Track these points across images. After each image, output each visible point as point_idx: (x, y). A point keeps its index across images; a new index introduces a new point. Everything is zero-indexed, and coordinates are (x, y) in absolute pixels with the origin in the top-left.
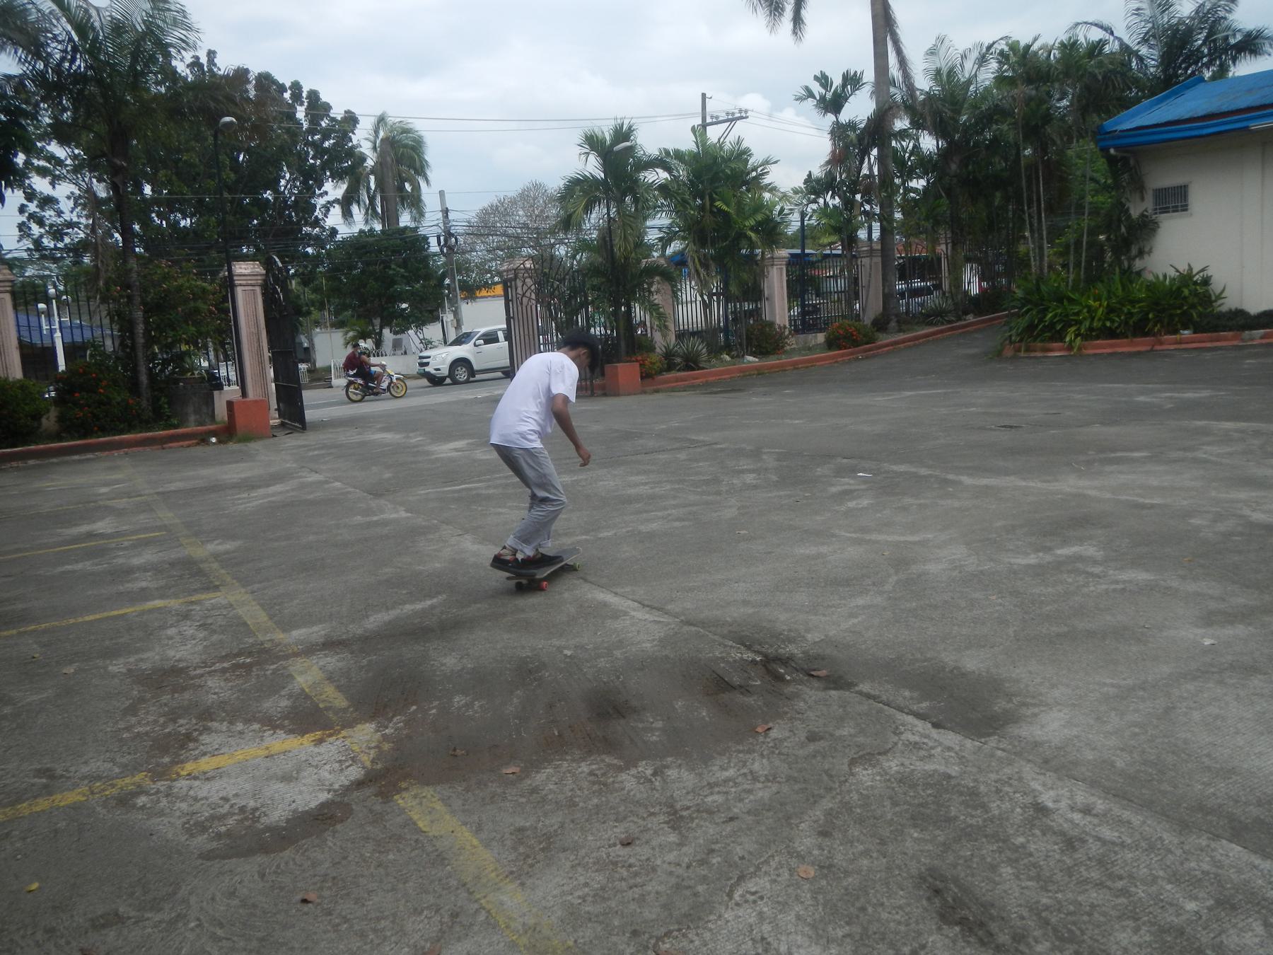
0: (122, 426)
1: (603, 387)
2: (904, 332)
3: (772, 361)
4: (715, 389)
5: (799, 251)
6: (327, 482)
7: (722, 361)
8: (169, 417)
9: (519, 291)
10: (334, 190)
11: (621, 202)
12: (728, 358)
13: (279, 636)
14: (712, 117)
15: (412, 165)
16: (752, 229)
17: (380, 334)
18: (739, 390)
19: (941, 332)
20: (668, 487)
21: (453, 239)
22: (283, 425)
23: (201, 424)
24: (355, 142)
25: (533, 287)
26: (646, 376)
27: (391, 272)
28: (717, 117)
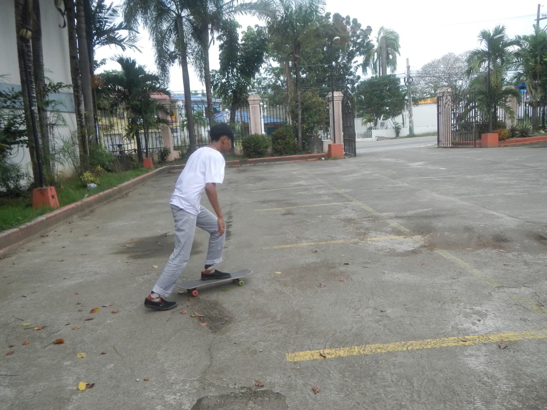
1: (480, 144)
7: (540, 133)
8: (308, 150)
9: (444, 102)
11: (494, 62)
13: (380, 214)
17: (377, 120)
20: (516, 181)
21: (411, 79)
22: (346, 154)
23: (319, 152)
24: (370, 39)
25: (450, 100)
26: (501, 139)
27: (383, 94)
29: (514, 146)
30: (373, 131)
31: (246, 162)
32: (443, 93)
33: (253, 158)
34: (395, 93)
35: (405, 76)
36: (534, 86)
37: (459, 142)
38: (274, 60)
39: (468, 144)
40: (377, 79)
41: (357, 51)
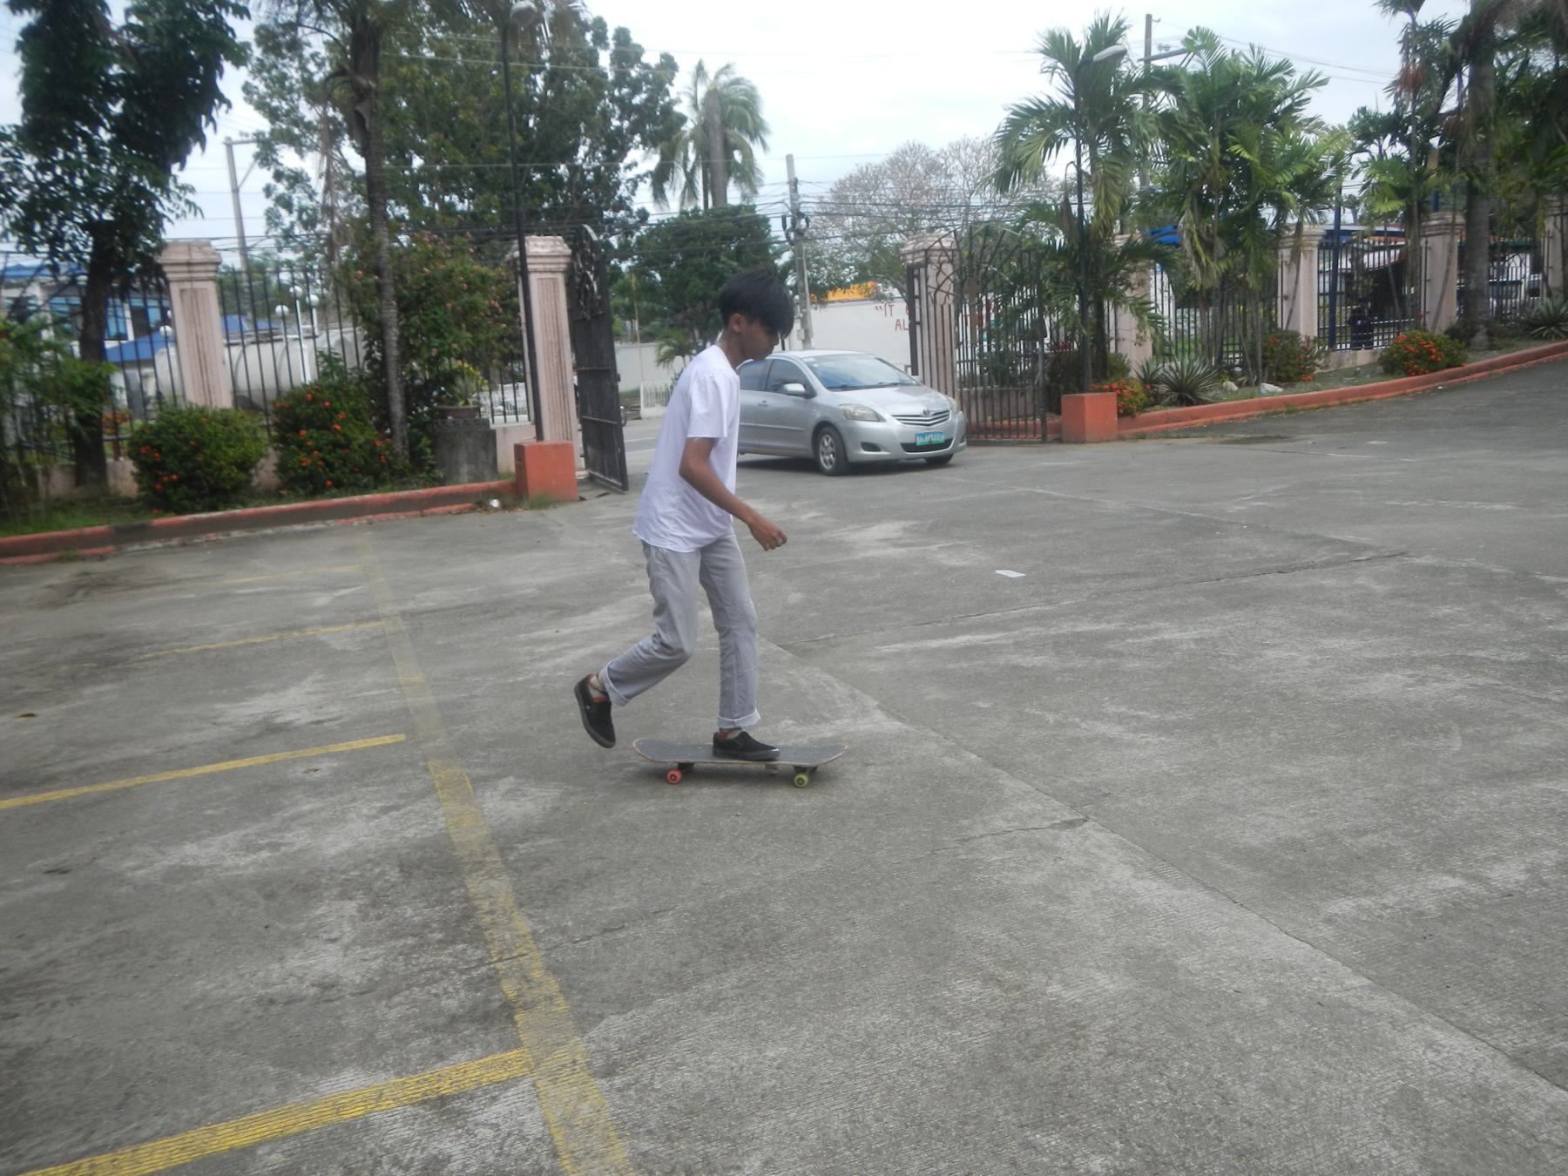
2: (1499, 349)
3: (1302, 392)
5: (1332, 227)
7: (1225, 390)
8: (433, 467)
9: (932, 282)
10: (641, 159)
12: (1232, 386)
14: (1160, 47)
15: (743, 126)
18: (1277, 438)
21: (803, 222)
22: (591, 478)
23: (477, 478)
27: (720, 266)
28: (1167, 48)
29: (1166, 435)
31: (139, 533)
32: (926, 251)
33: (181, 511)
35: (786, 210)
36: (1204, 235)
37: (982, 424)
39: (1018, 430)
41: (633, 131)
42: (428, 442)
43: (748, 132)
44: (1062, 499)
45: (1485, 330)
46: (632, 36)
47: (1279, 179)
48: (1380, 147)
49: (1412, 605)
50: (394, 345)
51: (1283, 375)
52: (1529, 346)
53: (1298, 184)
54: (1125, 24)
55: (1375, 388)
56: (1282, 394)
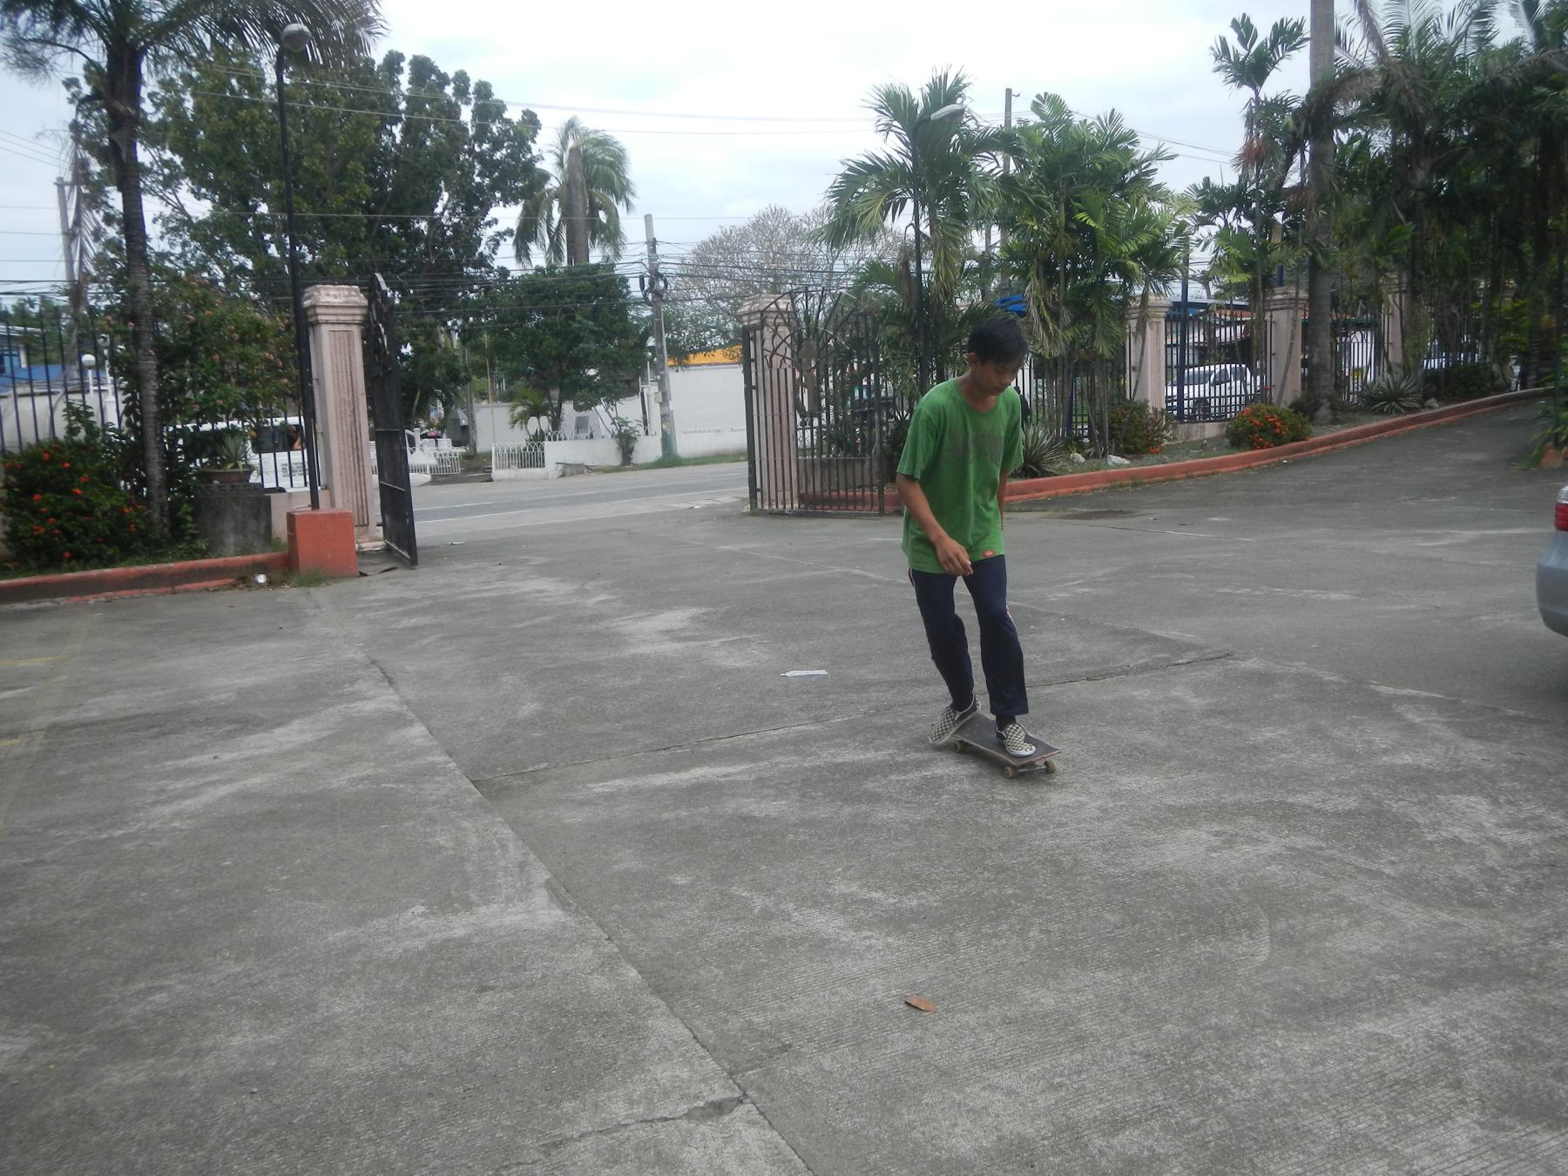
0: (110, 552)
2: (1342, 423)
3: (1149, 465)
4: (1079, 510)
6: (398, 721)
7: (1072, 462)
8: (194, 536)
9: (768, 345)
10: (506, 216)
12: (1080, 458)
16: (1134, 257)
17: (559, 410)
18: (1122, 512)
19: (1401, 424)
21: (662, 284)
22: (388, 549)
23: (245, 551)
24: (535, 152)
25: (789, 340)
27: (576, 325)
30: (547, 444)
32: (762, 312)
34: (612, 322)
38: (198, 196)
39: (855, 502)
40: (555, 275)
41: (493, 188)
42: (189, 509)
43: (614, 192)
44: (879, 582)
45: (1328, 404)
46: (493, 90)
47: (1124, 248)
48: (1226, 221)
49: (1229, 727)
50: (153, 400)
51: (1131, 447)
52: (1372, 420)
53: (1142, 253)
54: (964, 82)
55: (1219, 462)
56: (1129, 466)
